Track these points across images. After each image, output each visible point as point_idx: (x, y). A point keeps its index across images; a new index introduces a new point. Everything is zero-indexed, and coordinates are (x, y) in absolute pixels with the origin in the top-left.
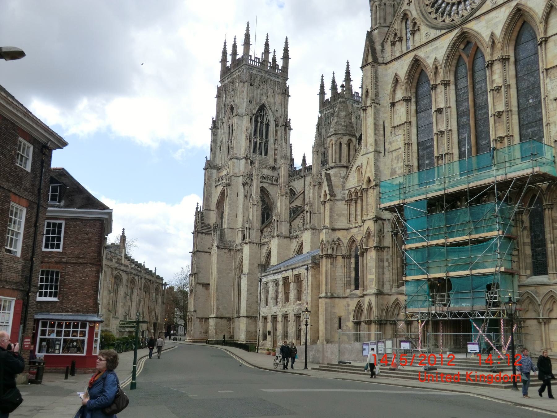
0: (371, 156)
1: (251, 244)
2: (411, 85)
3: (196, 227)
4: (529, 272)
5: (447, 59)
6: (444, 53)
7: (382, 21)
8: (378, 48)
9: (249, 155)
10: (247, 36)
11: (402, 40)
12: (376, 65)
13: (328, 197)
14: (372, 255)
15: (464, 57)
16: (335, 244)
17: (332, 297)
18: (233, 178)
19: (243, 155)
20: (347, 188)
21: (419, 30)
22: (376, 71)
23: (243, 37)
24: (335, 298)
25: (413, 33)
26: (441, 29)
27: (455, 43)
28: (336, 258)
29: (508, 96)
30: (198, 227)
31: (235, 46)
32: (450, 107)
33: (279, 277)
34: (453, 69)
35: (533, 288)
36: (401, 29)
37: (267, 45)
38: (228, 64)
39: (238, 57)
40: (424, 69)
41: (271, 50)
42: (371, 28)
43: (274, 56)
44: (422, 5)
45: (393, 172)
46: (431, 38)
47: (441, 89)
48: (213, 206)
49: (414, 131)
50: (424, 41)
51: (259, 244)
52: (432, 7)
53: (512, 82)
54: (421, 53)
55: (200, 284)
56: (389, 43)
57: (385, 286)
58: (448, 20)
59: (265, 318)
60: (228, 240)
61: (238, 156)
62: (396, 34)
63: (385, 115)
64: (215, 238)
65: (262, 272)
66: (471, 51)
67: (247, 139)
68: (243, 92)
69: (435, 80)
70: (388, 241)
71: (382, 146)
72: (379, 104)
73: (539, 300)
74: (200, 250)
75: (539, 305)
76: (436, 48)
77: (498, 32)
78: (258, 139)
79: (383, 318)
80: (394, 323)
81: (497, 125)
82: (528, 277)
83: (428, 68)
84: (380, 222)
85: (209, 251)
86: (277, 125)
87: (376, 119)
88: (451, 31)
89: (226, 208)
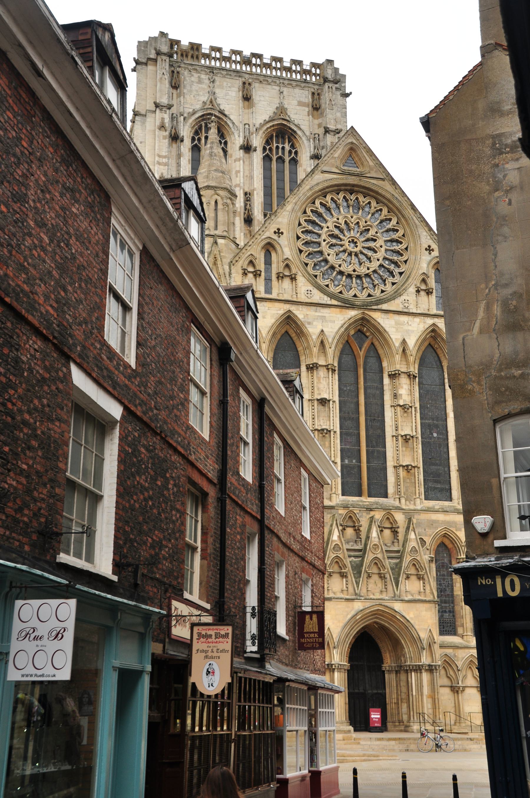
6: (335, 330)
11: (260, 275)
15: (355, 346)
21: (293, 278)
25: (280, 277)
26: (332, 296)
40: (293, 335)
50: (302, 298)
53: (417, 405)
54: (300, 313)
66: (366, 345)
73: (460, 664)
75: (459, 670)
76: (323, 318)
77: (411, 342)
83: (309, 339)
88: (348, 308)
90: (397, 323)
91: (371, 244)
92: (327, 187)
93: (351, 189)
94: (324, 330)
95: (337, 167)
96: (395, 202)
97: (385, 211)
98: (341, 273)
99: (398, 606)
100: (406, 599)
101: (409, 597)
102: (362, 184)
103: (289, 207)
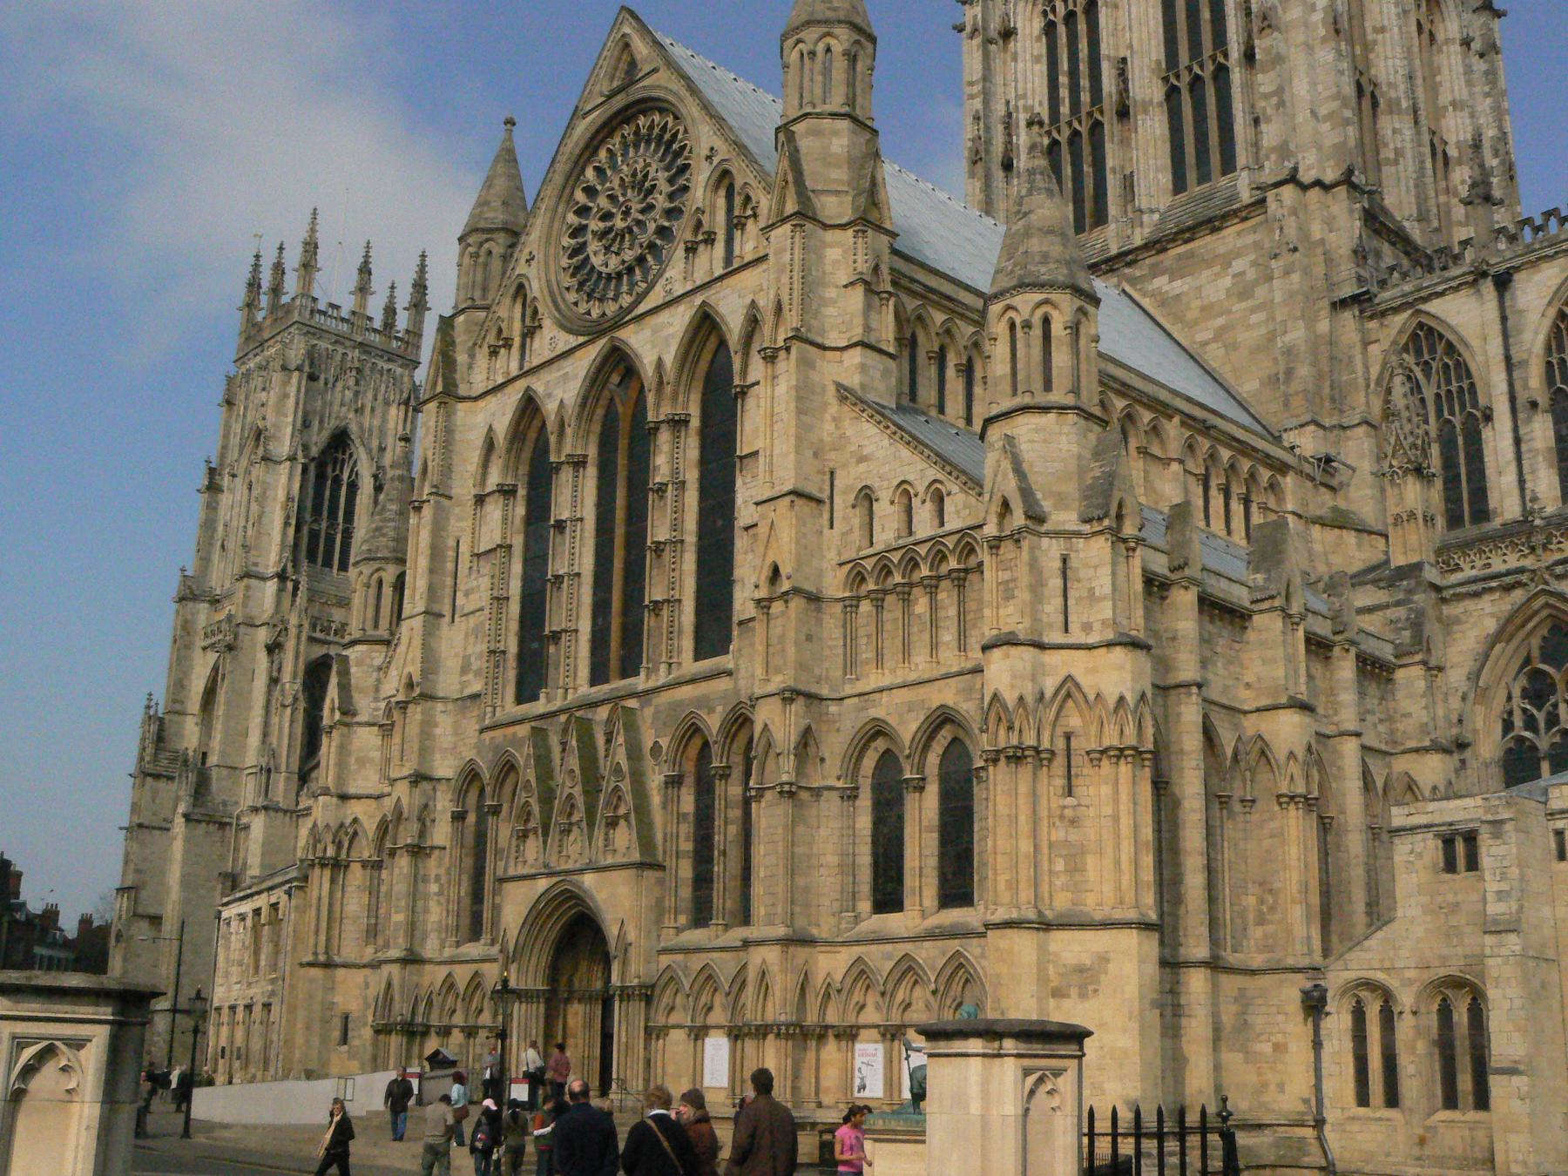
0: (418, 623)
1: (272, 813)
2: (518, 458)
3: (141, 759)
4: (682, 919)
5: (583, 404)
7: (478, 294)
8: (461, 358)
9: (290, 569)
10: (311, 247)
12: (451, 401)
13: (337, 716)
14: (403, 862)
15: (617, 401)
16: (347, 834)
17: (329, 965)
18: (242, 629)
19: (271, 570)
20: (383, 694)
21: (540, 327)
22: (449, 416)
23: (299, 249)
24: (337, 966)
25: (529, 333)
27: (599, 370)
28: (347, 867)
29: (679, 509)
30: (147, 758)
31: (279, 268)
32: (581, 519)
33: (246, 907)
34: (597, 427)
35: (679, 957)
36: (511, 319)
37: (365, 270)
38: (260, 316)
39: (285, 299)
41: (379, 283)
42: (455, 307)
43: (392, 297)
44: (552, 269)
45: (465, 669)
46: (558, 351)
47: (566, 475)
48: (194, 703)
49: (517, 567)
50: (548, 355)
51: (293, 812)
52: (573, 275)
53: (692, 476)
54: (538, 384)
55: (142, 917)
56: (485, 350)
57: (429, 942)
58: (595, 313)
59: (218, 1009)
60: (218, 800)
61: (261, 569)
62: (500, 331)
63: (460, 523)
64: (182, 793)
65: (224, 895)
67: (287, 524)
68: (286, 396)
69: (559, 452)
70: (441, 833)
71: (447, 601)
72: (450, 498)
74: (146, 823)
76: (565, 377)
77: (669, 360)
78: (324, 525)
79: (419, 1019)
80: (445, 1032)
81: (655, 572)
82: (679, 930)
84: (426, 785)
85: (164, 825)
86: (378, 488)
87: (438, 529)
89: (220, 709)
90: (654, 332)
91: (649, 200)
92: (592, 138)
93: (624, 116)
94: (566, 396)
95: (602, 95)
96: (670, 98)
97: (670, 119)
98: (609, 275)
99: (589, 880)
100: (603, 863)
101: (610, 861)
102: (631, 99)
103: (543, 207)
